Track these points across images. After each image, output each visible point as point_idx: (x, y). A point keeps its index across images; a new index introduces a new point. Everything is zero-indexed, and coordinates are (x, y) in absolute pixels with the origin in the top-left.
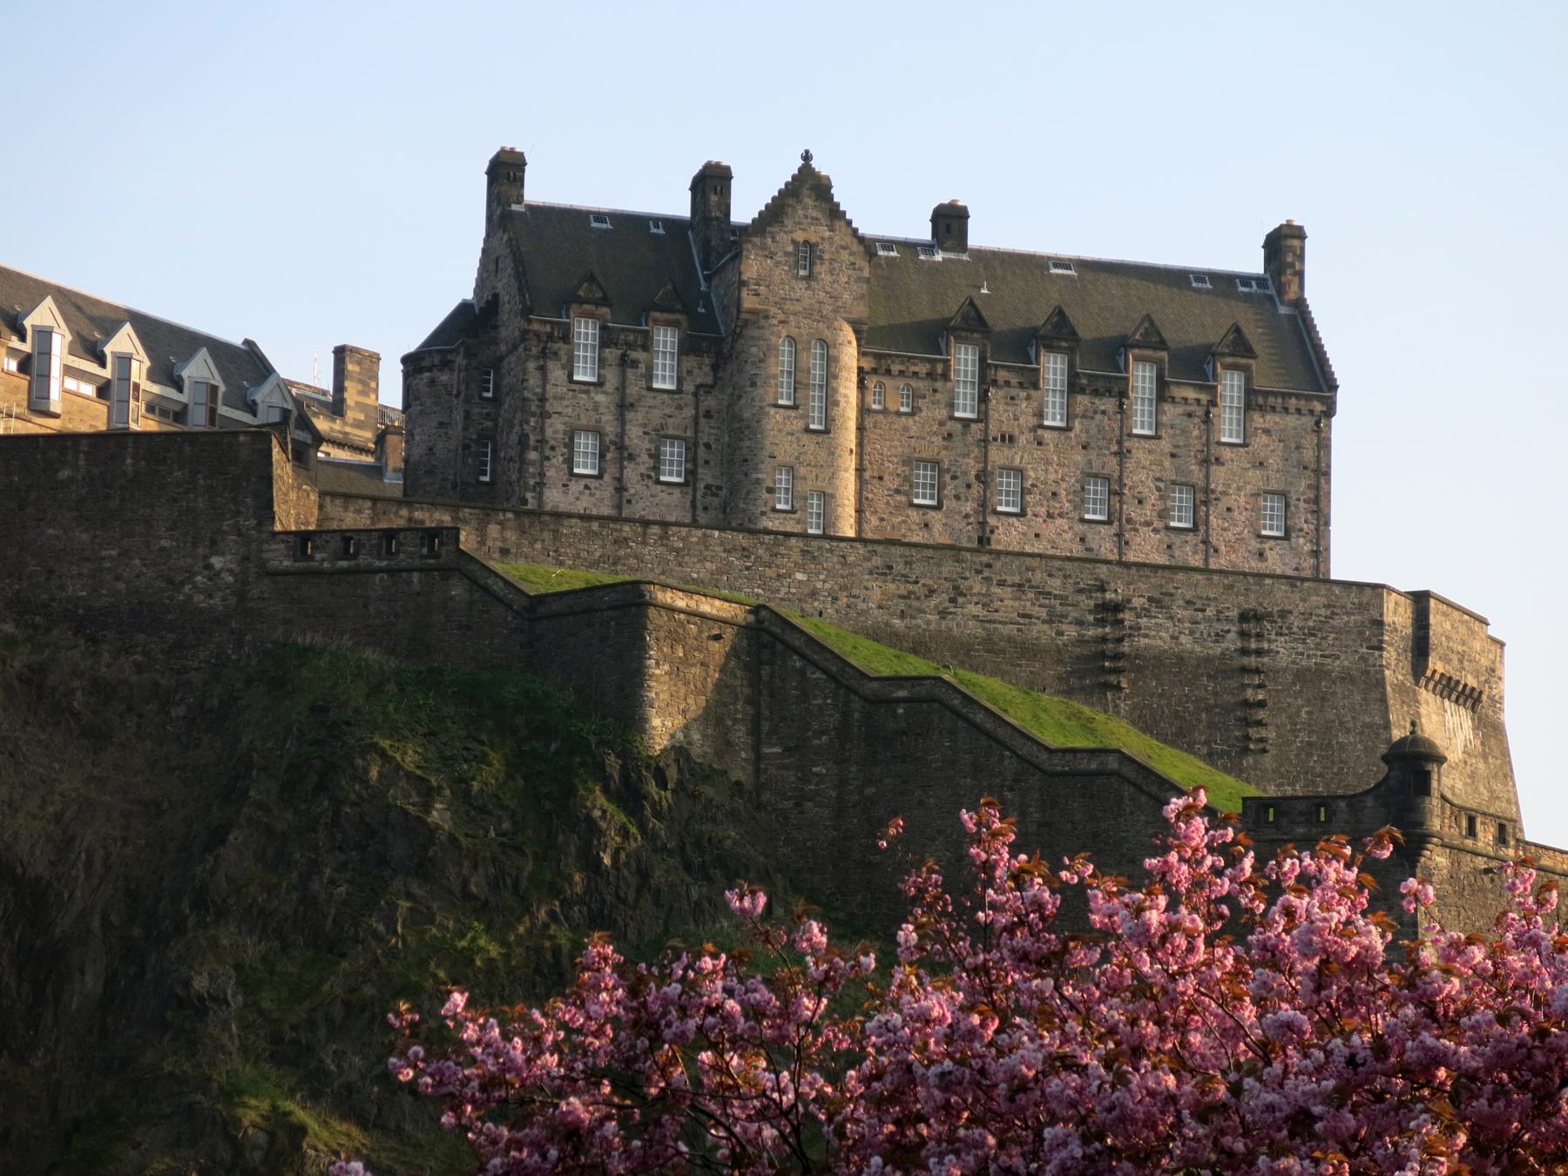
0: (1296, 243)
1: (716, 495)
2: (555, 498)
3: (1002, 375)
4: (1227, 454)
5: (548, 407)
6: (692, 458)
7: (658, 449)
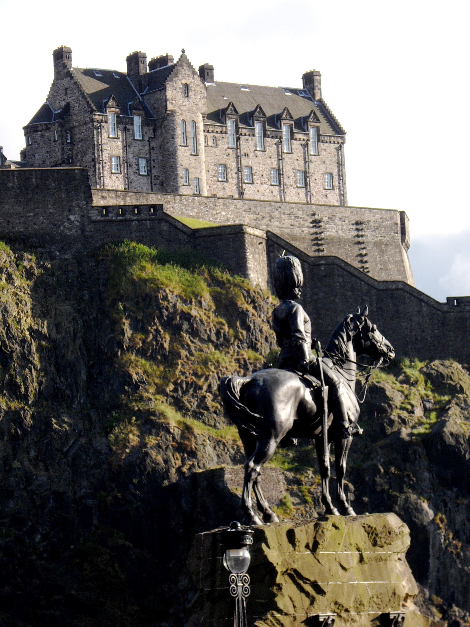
0: (318, 77)
1: (158, 179)
3: (244, 131)
4: (313, 158)
7: (138, 162)
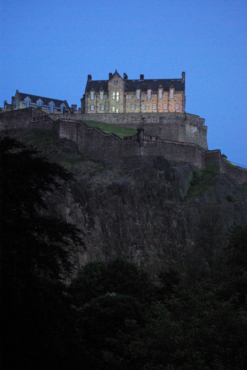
2: (89, 113)
4: (171, 100)
5: (88, 103)
6: (105, 107)
